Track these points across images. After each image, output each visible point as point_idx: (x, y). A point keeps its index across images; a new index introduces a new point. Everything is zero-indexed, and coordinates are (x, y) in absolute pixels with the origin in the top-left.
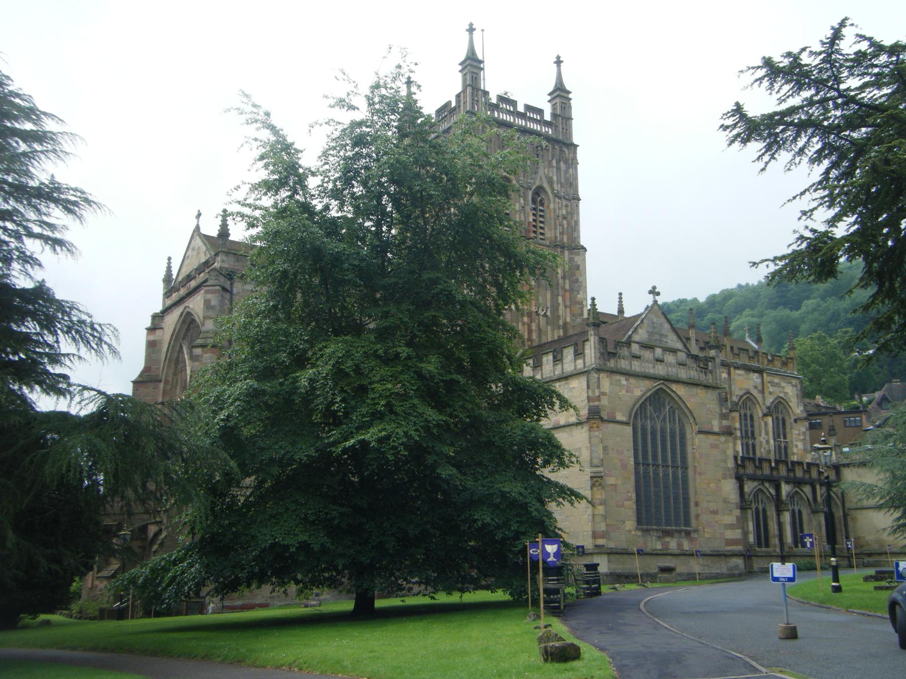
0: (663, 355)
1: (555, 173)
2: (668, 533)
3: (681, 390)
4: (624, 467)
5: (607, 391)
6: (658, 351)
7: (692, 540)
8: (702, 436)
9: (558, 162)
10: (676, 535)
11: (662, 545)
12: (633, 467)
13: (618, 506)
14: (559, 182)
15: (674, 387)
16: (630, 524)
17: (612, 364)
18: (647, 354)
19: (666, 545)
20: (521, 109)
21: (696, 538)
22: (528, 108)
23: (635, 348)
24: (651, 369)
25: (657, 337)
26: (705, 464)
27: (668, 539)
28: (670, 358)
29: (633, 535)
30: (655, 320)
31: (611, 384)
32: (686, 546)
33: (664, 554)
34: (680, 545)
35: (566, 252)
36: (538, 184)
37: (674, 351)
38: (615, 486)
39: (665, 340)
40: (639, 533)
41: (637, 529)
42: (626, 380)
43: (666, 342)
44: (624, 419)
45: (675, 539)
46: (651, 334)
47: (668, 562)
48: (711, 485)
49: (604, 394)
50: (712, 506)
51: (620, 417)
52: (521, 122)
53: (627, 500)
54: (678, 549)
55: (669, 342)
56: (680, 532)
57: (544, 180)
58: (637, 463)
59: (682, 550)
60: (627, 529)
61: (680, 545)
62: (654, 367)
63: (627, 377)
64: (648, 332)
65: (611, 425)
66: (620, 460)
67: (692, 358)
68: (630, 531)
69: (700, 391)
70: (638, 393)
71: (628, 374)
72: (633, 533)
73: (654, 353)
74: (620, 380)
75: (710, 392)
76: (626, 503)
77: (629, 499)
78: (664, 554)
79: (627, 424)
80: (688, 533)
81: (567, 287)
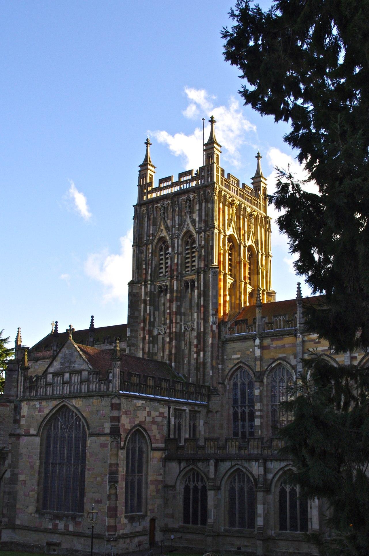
0: (70, 378)
1: (197, 215)
2: (58, 517)
3: (77, 403)
4: (32, 467)
5: (25, 414)
6: (67, 375)
7: (77, 524)
8: (94, 438)
9: (200, 205)
10: (65, 519)
11: (53, 525)
12: (38, 467)
13: (25, 495)
14: (200, 221)
15: (74, 402)
16: (32, 509)
17: (33, 394)
18: (59, 380)
19: (55, 526)
20: (175, 179)
21: (80, 522)
22: (181, 175)
23: (50, 377)
24: (58, 391)
25: (67, 365)
26: (94, 461)
27: (57, 522)
28: (76, 378)
29: (33, 517)
30: (67, 352)
31: (29, 408)
32: (71, 528)
33: (54, 531)
34: (66, 527)
35: (202, 275)
36: (185, 230)
37: (79, 372)
38: (25, 481)
39: (73, 365)
40: (37, 516)
41: (37, 511)
42: (39, 404)
43: (74, 367)
44: (35, 432)
45: (63, 522)
46: (62, 364)
47: (55, 539)
48: (98, 479)
49: (24, 417)
50: (97, 497)
51: (32, 431)
52: (175, 189)
53: (32, 491)
54: (64, 529)
55: (76, 366)
56: (67, 516)
57: (190, 224)
58: (47, 463)
59: (68, 530)
60: (29, 512)
61: (66, 527)
62: (63, 389)
63: (40, 401)
64: (61, 363)
65: (27, 438)
66: (30, 463)
67: (94, 374)
68: (31, 514)
69: (96, 401)
70: (47, 411)
71: (41, 399)
72: (33, 515)
73: (63, 378)
74: (35, 405)
75: (106, 399)
76: (31, 493)
77: (33, 491)
78: (54, 531)
79: (37, 435)
80: (74, 518)
81: (202, 304)
